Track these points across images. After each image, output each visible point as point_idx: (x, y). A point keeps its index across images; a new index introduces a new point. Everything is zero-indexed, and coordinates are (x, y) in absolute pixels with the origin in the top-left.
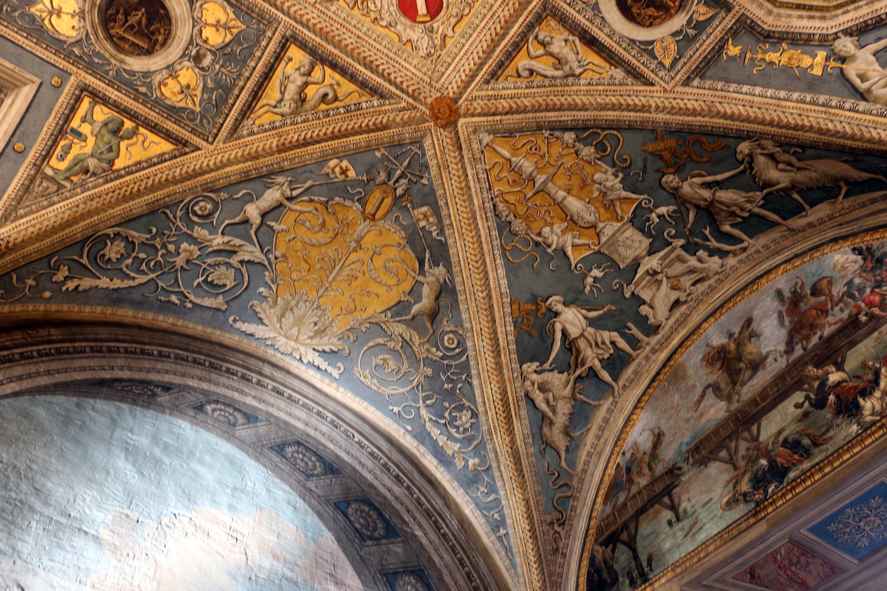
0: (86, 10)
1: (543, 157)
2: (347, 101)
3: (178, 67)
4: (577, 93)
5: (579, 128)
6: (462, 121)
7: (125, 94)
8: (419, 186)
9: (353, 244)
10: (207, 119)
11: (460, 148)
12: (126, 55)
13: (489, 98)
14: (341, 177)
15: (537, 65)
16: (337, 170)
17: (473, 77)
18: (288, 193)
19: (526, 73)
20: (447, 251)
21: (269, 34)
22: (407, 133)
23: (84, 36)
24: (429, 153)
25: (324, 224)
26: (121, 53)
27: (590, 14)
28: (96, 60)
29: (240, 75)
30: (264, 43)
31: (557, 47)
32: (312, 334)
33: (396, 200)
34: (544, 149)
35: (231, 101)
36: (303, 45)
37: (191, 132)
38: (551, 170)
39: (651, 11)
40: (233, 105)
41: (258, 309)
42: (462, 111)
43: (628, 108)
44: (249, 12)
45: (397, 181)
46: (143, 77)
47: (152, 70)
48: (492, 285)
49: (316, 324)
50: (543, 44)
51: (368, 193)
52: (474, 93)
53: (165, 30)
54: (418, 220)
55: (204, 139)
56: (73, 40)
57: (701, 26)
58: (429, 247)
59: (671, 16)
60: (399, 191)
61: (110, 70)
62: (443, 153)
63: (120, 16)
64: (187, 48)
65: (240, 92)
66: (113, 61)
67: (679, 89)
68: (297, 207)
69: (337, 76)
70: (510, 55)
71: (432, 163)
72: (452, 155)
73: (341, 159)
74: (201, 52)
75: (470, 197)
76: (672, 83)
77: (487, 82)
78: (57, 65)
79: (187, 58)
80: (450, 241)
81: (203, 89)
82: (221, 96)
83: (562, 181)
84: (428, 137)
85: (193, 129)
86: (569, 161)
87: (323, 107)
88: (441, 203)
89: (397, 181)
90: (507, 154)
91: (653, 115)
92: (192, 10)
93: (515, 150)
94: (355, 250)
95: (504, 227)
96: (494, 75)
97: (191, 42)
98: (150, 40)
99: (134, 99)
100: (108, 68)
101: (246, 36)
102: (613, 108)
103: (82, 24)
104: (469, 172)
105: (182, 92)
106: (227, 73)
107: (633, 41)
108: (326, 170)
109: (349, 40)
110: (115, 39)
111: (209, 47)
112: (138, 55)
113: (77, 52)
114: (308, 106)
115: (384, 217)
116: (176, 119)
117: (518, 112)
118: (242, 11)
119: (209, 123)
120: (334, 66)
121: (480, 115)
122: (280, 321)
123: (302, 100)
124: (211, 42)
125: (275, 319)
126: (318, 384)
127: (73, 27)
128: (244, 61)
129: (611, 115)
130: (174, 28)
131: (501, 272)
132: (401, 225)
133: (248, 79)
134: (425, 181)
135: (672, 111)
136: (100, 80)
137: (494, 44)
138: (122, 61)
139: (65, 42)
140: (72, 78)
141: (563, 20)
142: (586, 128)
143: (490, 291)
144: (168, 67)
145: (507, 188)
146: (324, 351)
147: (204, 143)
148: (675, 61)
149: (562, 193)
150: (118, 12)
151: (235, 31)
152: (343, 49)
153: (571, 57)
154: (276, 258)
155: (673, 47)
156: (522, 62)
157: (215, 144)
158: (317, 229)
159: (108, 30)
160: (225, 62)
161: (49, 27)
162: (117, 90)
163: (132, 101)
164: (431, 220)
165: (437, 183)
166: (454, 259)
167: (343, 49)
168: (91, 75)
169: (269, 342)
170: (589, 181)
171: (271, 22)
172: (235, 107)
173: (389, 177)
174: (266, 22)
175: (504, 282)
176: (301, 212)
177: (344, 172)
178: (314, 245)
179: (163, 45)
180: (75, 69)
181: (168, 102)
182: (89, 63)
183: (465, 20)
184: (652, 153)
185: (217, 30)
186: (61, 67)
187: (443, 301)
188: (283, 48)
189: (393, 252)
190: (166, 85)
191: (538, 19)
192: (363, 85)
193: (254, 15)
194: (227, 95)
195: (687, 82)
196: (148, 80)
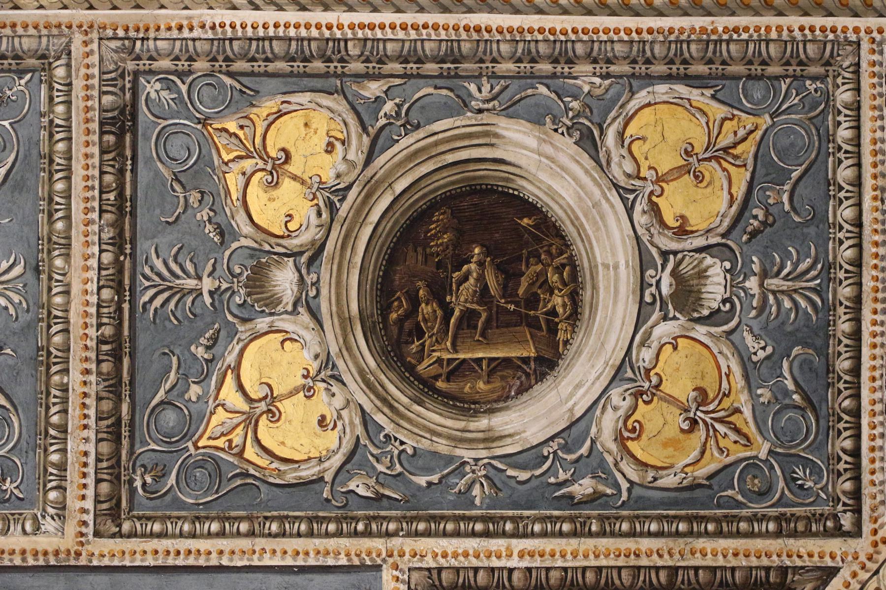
0: (334, 349)
3: (646, 355)
7: (544, 534)
10: (806, 463)
12: (491, 411)
21: (844, 96)
23: (359, 430)
26: (476, 414)
28: (422, 481)
29: (829, 267)
30: (844, 133)
35: (844, 364)
37: (778, 534)
40: (856, 371)
44: (757, 69)
46: (568, 450)
47: (578, 412)
53: (559, 269)
55: (827, 534)
56: (337, 461)
61: (470, 487)
63: (426, 309)
64: (643, 285)
65: (857, 320)
66: (467, 454)
74: (686, 268)
78: (330, 562)
79: (656, 315)
81: (746, 377)
82: (806, 365)
85: (778, 519)
92: (603, 166)
97: (644, 262)
98: (533, 324)
99: (574, 534)
100: (462, 484)
101: (785, 142)
103: (339, 402)
105: (694, 422)
110: (440, 384)
111: (700, 242)
112: (521, 391)
113: (362, 491)
116: (717, 520)
118: (736, 78)
119: (816, 472)
124: (696, 222)
127: (322, 422)
128: (818, 218)
130: (579, 247)
133: (858, 262)
136: (457, 534)
138: (490, 439)
139: (321, 479)
140: (387, 574)
144: (617, 375)
147: (835, 545)
150: (415, 303)
151: (747, 149)
157: (867, 527)
159: (411, 369)
160: (765, 257)
161: (263, 462)
162: (515, 535)
163: (574, 542)
168: (427, 534)
172: (865, 374)
174: (814, 70)
179: (574, 316)
180: (378, 544)
181: (669, 481)
182: (407, 502)
185: (699, 178)
186: (343, 561)
190: (637, 432)
193: (774, 70)
194: (822, 350)
196: (584, 450)
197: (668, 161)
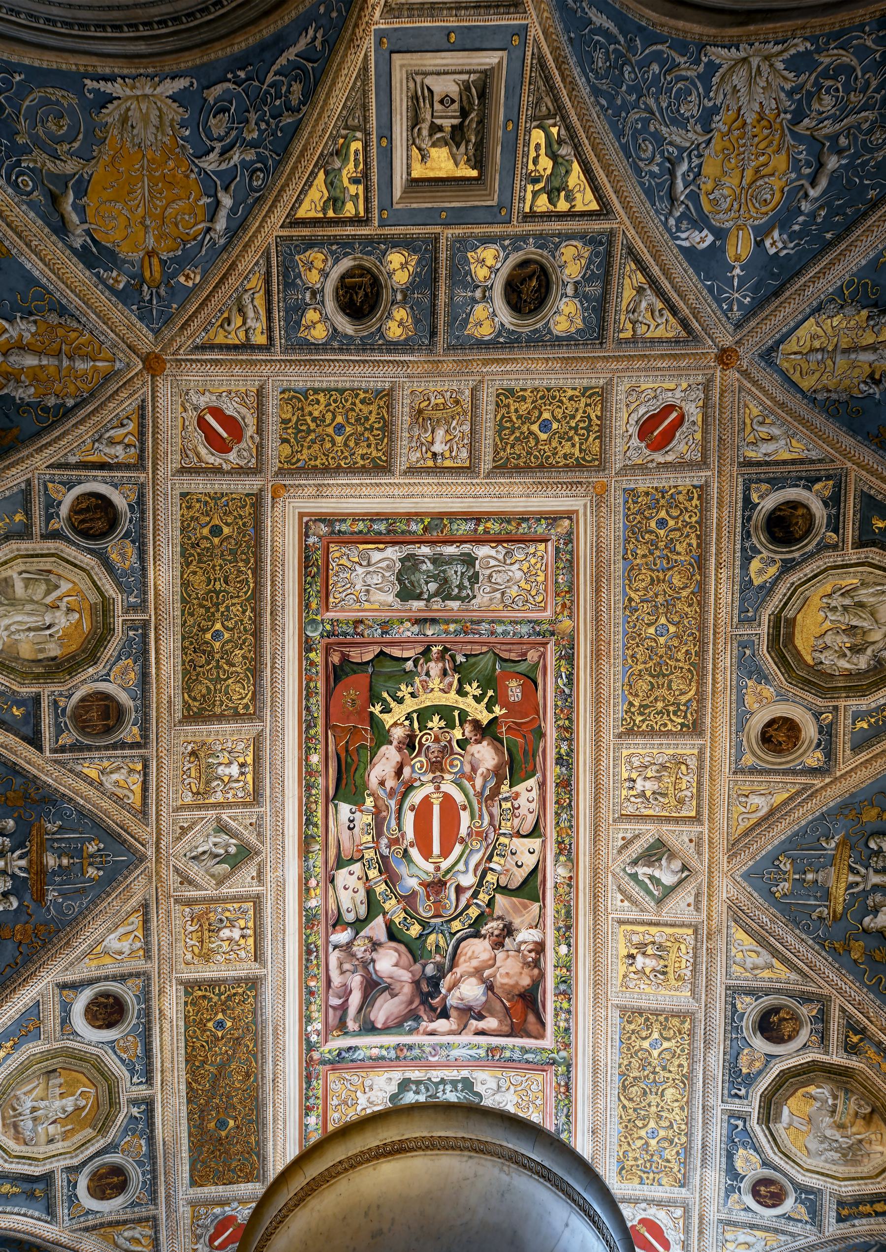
1: (76, 378)
2: (214, 329)
4: (87, 432)
5: (69, 412)
6: (141, 366)
8: (136, 301)
9: (148, 222)
11: (129, 347)
13: (135, 392)
14: (187, 272)
15: (122, 431)
16: (192, 276)
17: (154, 398)
18: (212, 234)
19: (125, 421)
20: (84, 263)
22: (167, 334)
24: (145, 330)
25: (177, 225)
27: (116, 480)
31: (119, 450)
32: (130, 113)
33: (143, 281)
34: (79, 384)
36: (260, 348)
38: (63, 373)
39: (84, 506)
41: (181, 110)
42: (145, 372)
43: (49, 444)
45: (151, 294)
48: (33, 256)
49: (132, 126)
50: (128, 446)
51: (163, 272)
52: (145, 389)
54: (119, 275)
57: (49, 517)
58: (97, 257)
59: (70, 511)
60: (145, 288)
62: (137, 336)
67: (29, 475)
68: (200, 226)
69: (230, 342)
70: (142, 426)
71: (139, 324)
72: (131, 338)
73: (195, 285)
75: (99, 317)
76: (36, 475)
77: (143, 401)
80: (88, 273)
83: (52, 369)
84: (152, 340)
86: (57, 386)
87: (226, 315)
88: (114, 299)
89: (151, 294)
90: (99, 364)
91: (31, 450)
93: (95, 369)
94: (144, 217)
95: (62, 311)
96: (142, 407)
102: (58, 438)
104: (112, 335)
106: (294, 296)
107: (80, 483)
108: (198, 270)
109: (237, 370)
114: (235, 308)
115: (143, 260)
117: (112, 395)
120: (235, 348)
121: (133, 377)
122: (160, 109)
123: (241, 310)
125: (165, 110)
126: (94, 61)
129: (56, 433)
131: (36, 273)
132: (127, 262)
134: (134, 307)
135: (22, 460)
137: (155, 426)
141: (127, 467)
142: (64, 415)
143: (32, 251)
145: (82, 340)
146: (111, 102)
148: (46, 488)
149: (45, 362)
152: (237, 362)
153: (107, 450)
154: (192, 171)
155: (54, 496)
156: (131, 426)
158: (179, 217)
164: (111, 281)
165: (127, 312)
166: (75, 259)
167: (237, 362)
169: (157, 79)
170: (34, 383)
171: (286, 350)
173: (158, 293)
175: (28, 266)
176: (196, 224)
177: (187, 277)
178: (173, 201)
183: (180, 429)
184: (11, 428)
187: (56, 218)
188: (270, 338)
189: (117, 236)
191: (141, 457)
192: (212, 347)
195: (28, 482)
197: (319, 326)
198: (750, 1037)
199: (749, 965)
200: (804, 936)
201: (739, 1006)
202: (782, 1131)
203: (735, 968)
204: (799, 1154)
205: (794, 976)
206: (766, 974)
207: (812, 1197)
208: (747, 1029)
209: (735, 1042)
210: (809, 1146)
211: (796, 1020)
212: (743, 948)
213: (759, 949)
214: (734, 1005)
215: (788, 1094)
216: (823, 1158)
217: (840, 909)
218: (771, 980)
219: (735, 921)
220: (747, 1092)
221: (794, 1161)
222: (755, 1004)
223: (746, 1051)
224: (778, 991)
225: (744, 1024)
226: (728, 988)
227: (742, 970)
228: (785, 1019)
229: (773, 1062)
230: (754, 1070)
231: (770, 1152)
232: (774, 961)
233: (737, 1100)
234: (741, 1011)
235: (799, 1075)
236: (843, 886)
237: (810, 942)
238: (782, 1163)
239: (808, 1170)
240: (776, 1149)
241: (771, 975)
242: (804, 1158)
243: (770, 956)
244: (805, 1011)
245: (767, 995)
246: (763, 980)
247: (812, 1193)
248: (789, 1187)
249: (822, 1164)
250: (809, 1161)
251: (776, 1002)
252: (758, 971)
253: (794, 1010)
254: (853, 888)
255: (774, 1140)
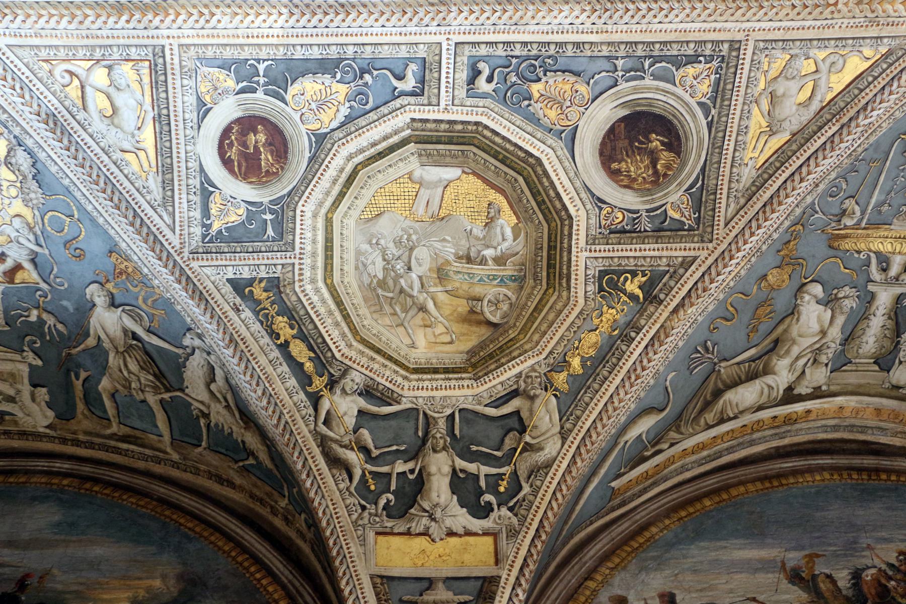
198: (617, 96)
199: (781, 87)
200: (822, 187)
201: (691, 70)
202: (403, 169)
203: (781, 58)
204: (361, 203)
205: (747, 174)
206: (757, 120)
207: (270, 232)
208: (636, 90)
209: (607, 65)
210: (384, 221)
211: (655, 183)
212: (823, 75)
213: (815, 106)
214: (693, 60)
215: (490, 176)
216: (365, 247)
217: (847, 245)
218: (743, 131)
219: (889, 53)
220: (485, 96)
221: (342, 195)
222: (692, 102)
223: (583, 89)
224: (717, 147)
225: (648, 82)
226: (735, 45)
227: (772, 74)
228: (654, 163)
229: (559, 145)
230: (537, 108)
231: (352, 147)
232: (786, 137)
233: (463, 75)
234: (678, 75)
235: (535, 194)
236: (886, 247)
237: (809, 199)
238: (332, 172)
239: (329, 222)
240: (360, 158)
241: (753, 131)
242: (355, 214)
243: (795, 128)
244: (673, 198)
245: (710, 125)
246: (746, 115)
247: (280, 234)
248: (280, 189)
249: (350, 245)
250: (351, 222)
251: (694, 142)
252: (765, 104)
253: (675, 177)
254: (879, 262)
255: (381, 155)
